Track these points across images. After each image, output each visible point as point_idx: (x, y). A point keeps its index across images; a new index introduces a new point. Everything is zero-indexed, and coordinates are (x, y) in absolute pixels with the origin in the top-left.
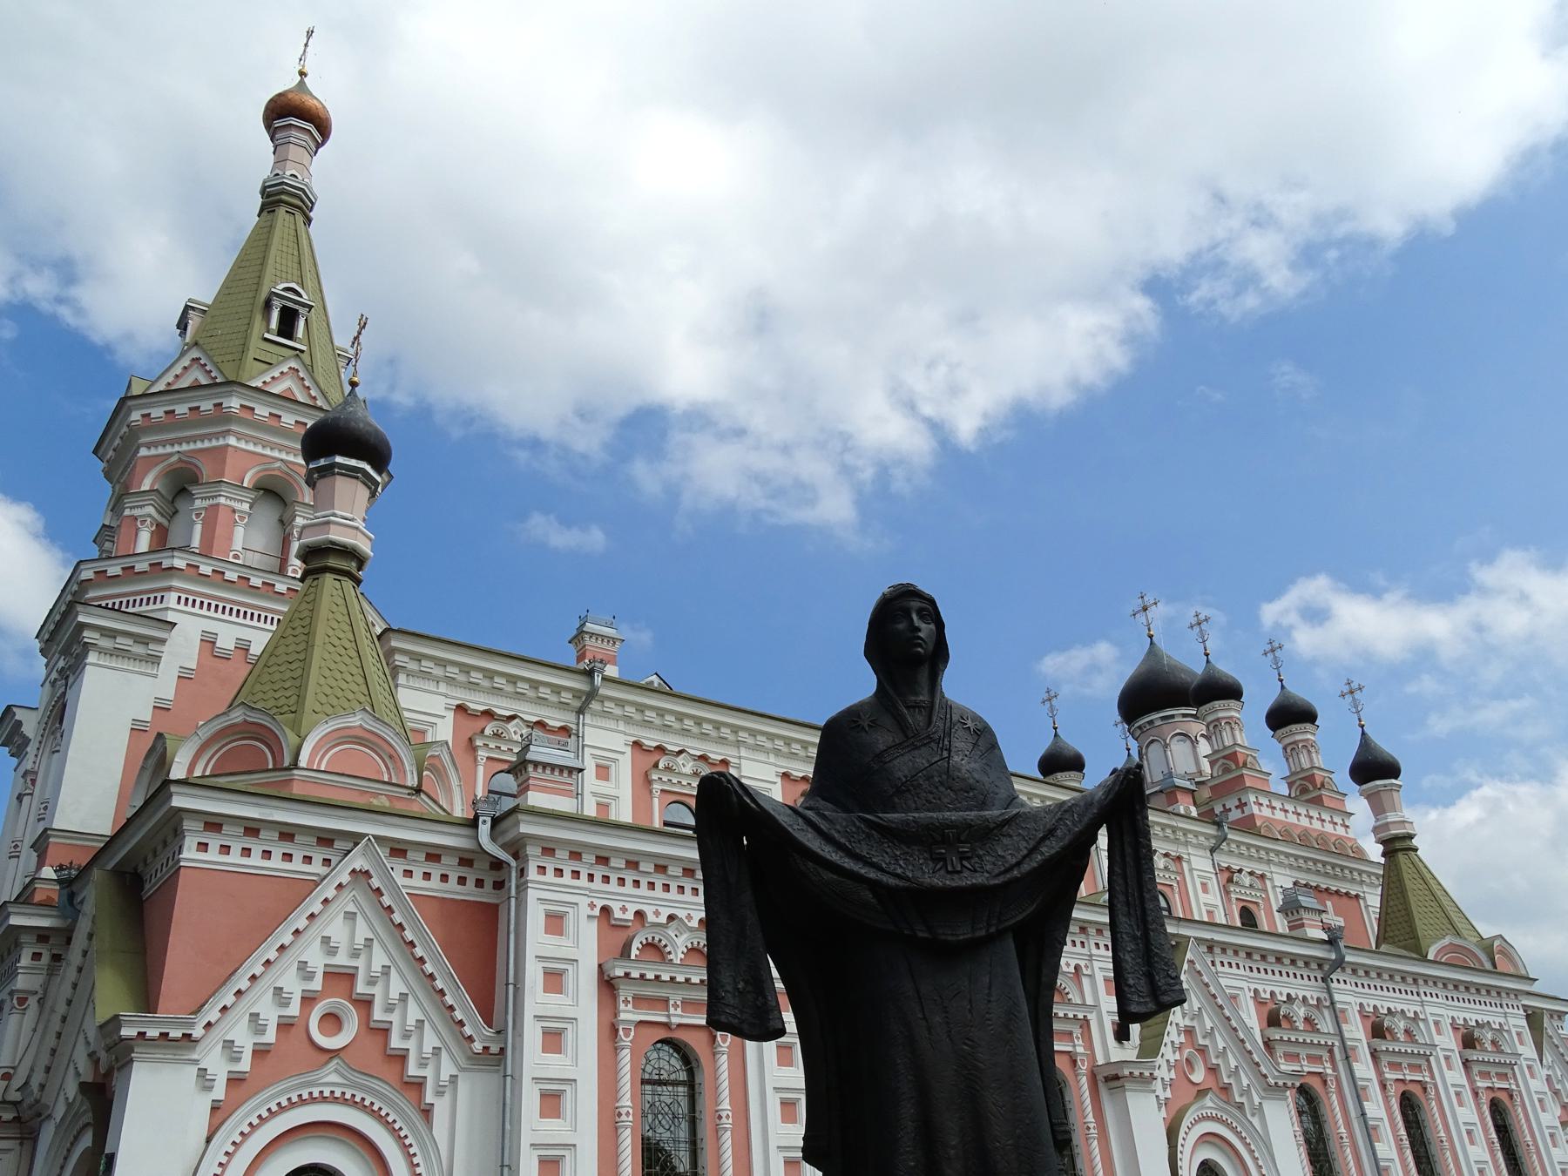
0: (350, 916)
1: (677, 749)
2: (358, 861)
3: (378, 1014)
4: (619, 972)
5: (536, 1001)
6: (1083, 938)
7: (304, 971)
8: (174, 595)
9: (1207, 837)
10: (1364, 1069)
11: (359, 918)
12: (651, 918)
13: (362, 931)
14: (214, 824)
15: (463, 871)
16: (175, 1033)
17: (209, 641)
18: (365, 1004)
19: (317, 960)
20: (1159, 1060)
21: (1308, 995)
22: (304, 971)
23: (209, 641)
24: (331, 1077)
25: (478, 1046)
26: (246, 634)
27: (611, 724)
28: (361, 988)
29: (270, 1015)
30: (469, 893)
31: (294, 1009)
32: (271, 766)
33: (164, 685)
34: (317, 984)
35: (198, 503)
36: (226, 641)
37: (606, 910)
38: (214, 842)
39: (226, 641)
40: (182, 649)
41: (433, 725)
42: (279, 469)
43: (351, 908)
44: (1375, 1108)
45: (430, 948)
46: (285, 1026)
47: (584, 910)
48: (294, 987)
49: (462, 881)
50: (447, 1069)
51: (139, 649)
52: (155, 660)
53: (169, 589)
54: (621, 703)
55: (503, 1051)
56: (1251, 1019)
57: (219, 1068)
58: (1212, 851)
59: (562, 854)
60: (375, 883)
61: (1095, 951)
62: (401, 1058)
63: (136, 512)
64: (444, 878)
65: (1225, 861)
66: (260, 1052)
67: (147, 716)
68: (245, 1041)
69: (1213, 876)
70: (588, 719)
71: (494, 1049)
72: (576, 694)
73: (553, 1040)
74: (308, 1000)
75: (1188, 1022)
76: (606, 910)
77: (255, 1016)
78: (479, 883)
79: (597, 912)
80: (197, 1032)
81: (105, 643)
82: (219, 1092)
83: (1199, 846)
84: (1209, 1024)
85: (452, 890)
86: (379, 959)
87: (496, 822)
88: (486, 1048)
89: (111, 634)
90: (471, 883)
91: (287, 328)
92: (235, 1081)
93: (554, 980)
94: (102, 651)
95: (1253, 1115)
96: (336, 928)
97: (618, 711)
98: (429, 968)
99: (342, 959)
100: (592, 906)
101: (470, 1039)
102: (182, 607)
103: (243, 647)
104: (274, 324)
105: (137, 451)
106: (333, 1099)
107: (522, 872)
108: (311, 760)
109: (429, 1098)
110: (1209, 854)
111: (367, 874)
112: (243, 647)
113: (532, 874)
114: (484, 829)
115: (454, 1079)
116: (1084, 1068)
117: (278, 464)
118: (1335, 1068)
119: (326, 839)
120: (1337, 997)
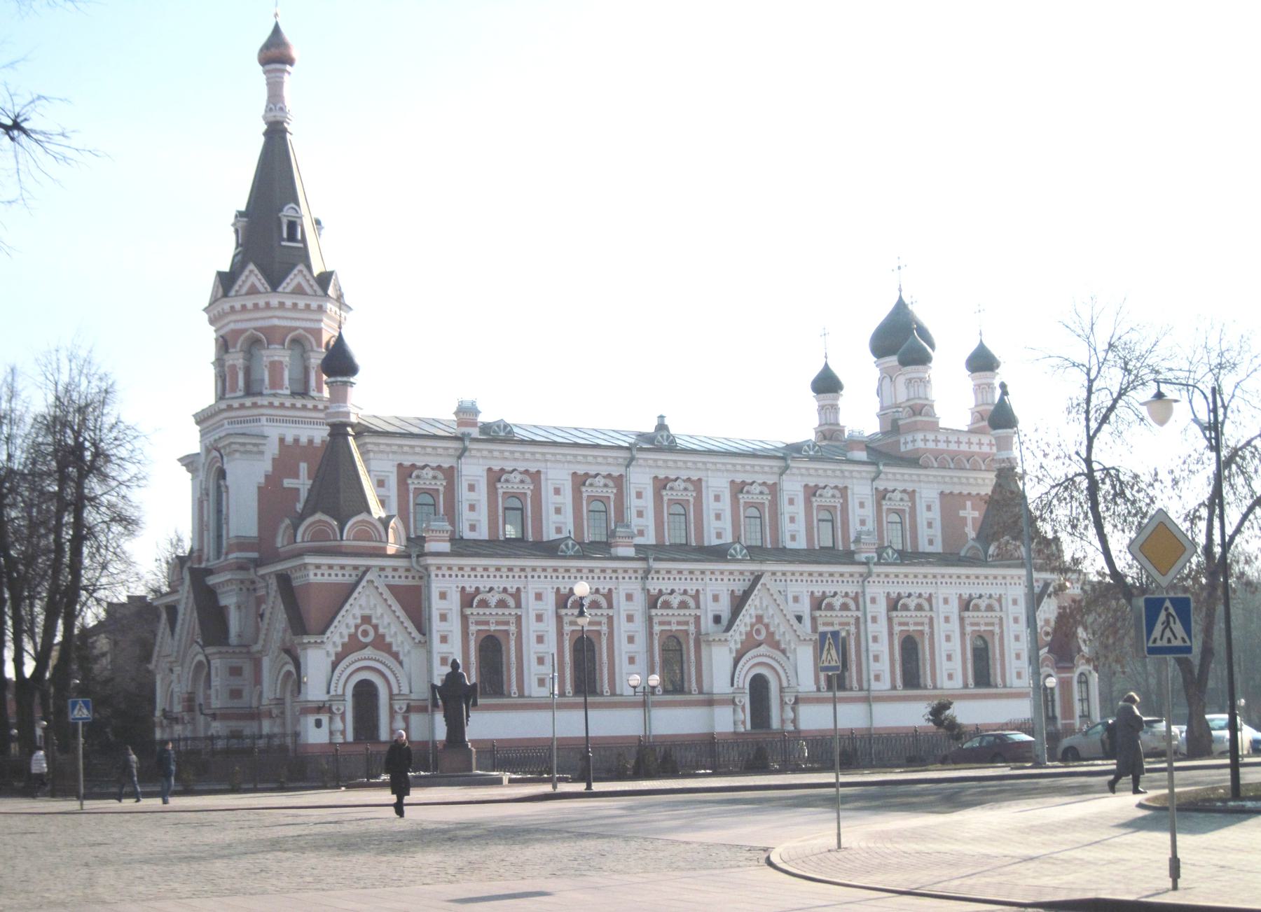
0: (368, 596)
1: (511, 469)
2: (368, 577)
3: (381, 630)
4: (469, 613)
5: (437, 626)
6: (703, 576)
7: (354, 617)
8: (264, 419)
9: (867, 472)
10: (881, 628)
11: (371, 597)
12: (482, 589)
13: (372, 602)
14: (318, 567)
15: (407, 574)
16: (319, 641)
17: (282, 440)
18: (376, 627)
19: (358, 612)
20: (731, 632)
21: (849, 591)
22: (354, 617)
23: (282, 440)
24: (368, 652)
25: (417, 641)
26: (296, 432)
27: (475, 461)
28: (374, 621)
29: (346, 632)
30: (410, 582)
31: (353, 630)
32: (332, 538)
33: (266, 466)
34: (359, 621)
35: (265, 359)
36: (289, 439)
37: (463, 588)
38: (319, 572)
39: (289, 439)
40: (272, 449)
41: (388, 476)
42: (300, 334)
43: (368, 593)
44: (882, 648)
45: (396, 607)
46: (350, 636)
47: (454, 589)
48: (352, 622)
49: (407, 577)
50: (407, 647)
51: (255, 449)
52: (262, 453)
53: (263, 415)
54: (478, 450)
55: (426, 642)
56: (805, 608)
57: (332, 651)
58: (873, 480)
59: (444, 568)
60: (376, 584)
61: (708, 581)
62: (390, 645)
63: (236, 362)
64: (400, 577)
65: (881, 485)
66: (344, 645)
67: (262, 480)
68: (339, 641)
69: (870, 497)
70: (463, 459)
71: (423, 641)
72: (456, 449)
73: (444, 639)
74: (357, 627)
75: (760, 612)
76: (463, 588)
77: (341, 633)
78: (413, 578)
79: (460, 589)
80: (325, 640)
81: (242, 449)
82: (333, 658)
83: (862, 478)
84: (771, 612)
85: (403, 582)
86: (379, 611)
87: (418, 556)
88: (420, 642)
89: (244, 444)
90: (410, 579)
91: (292, 237)
92: (337, 654)
93: (443, 618)
94: (242, 452)
95: (790, 652)
96: (363, 601)
97: (478, 454)
98: (397, 614)
99: (367, 612)
100: (457, 587)
101: (414, 638)
102: (270, 424)
103: (296, 440)
104: (285, 235)
105: (228, 323)
106: (369, 659)
107: (429, 576)
108: (347, 536)
109: (401, 657)
110: (870, 482)
111: (372, 582)
112: (296, 440)
113: (433, 576)
114: (414, 560)
115: (409, 652)
116: (692, 638)
117: (297, 332)
118: (858, 627)
119: (356, 568)
120: (868, 590)
